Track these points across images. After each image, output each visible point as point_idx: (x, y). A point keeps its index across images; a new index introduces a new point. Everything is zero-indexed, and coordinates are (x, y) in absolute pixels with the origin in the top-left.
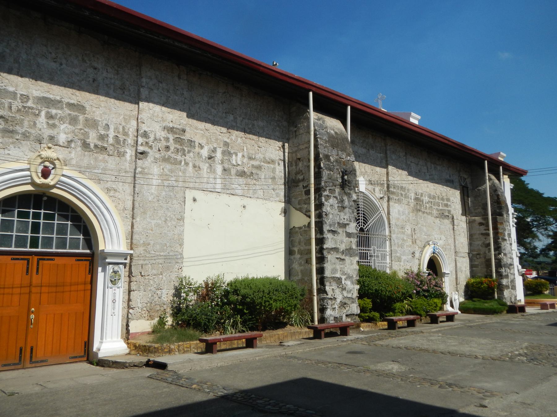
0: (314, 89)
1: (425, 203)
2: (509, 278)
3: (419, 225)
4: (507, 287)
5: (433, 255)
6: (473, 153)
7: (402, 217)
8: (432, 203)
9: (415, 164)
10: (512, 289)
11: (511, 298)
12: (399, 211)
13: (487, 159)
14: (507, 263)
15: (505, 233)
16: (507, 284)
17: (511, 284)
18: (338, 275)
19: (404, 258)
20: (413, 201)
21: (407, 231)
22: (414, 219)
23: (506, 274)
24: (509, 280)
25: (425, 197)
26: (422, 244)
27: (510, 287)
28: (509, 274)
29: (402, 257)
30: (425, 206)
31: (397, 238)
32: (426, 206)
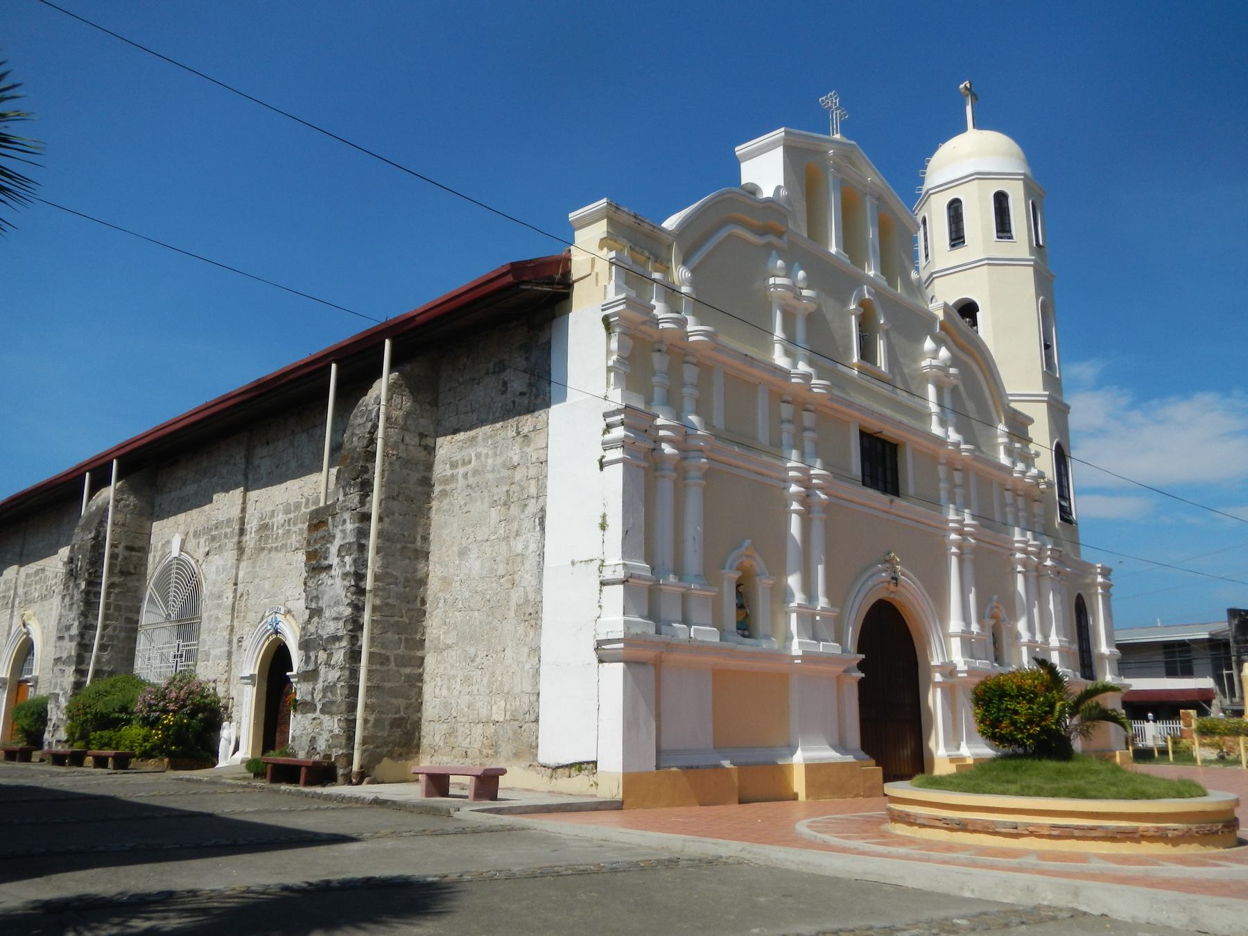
0: (86, 468)
1: (278, 528)
2: (321, 679)
3: (257, 581)
4: (308, 707)
5: (274, 636)
6: (291, 377)
7: (222, 576)
8: (292, 523)
9: (270, 456)
10: (322, 712)
11: (313, 740)
12: (217, 568)
13: (331, 359)
14: (321, 637)
15: (328, 548)
16: (309, 698)
17: (324, 697)
18: (57, 691)
19: (213, 653)
20: (253, 535)
21: (225, 600)
22: (249, 572)
23: (311, 667)
24: (320, 686)
25: (278, 516)
26: (257, 619)
27: (319, 706)
28: (322, 669)
29: (211, 651)
30: (275, 536)
31: (210, 617)
32: (278, 534)
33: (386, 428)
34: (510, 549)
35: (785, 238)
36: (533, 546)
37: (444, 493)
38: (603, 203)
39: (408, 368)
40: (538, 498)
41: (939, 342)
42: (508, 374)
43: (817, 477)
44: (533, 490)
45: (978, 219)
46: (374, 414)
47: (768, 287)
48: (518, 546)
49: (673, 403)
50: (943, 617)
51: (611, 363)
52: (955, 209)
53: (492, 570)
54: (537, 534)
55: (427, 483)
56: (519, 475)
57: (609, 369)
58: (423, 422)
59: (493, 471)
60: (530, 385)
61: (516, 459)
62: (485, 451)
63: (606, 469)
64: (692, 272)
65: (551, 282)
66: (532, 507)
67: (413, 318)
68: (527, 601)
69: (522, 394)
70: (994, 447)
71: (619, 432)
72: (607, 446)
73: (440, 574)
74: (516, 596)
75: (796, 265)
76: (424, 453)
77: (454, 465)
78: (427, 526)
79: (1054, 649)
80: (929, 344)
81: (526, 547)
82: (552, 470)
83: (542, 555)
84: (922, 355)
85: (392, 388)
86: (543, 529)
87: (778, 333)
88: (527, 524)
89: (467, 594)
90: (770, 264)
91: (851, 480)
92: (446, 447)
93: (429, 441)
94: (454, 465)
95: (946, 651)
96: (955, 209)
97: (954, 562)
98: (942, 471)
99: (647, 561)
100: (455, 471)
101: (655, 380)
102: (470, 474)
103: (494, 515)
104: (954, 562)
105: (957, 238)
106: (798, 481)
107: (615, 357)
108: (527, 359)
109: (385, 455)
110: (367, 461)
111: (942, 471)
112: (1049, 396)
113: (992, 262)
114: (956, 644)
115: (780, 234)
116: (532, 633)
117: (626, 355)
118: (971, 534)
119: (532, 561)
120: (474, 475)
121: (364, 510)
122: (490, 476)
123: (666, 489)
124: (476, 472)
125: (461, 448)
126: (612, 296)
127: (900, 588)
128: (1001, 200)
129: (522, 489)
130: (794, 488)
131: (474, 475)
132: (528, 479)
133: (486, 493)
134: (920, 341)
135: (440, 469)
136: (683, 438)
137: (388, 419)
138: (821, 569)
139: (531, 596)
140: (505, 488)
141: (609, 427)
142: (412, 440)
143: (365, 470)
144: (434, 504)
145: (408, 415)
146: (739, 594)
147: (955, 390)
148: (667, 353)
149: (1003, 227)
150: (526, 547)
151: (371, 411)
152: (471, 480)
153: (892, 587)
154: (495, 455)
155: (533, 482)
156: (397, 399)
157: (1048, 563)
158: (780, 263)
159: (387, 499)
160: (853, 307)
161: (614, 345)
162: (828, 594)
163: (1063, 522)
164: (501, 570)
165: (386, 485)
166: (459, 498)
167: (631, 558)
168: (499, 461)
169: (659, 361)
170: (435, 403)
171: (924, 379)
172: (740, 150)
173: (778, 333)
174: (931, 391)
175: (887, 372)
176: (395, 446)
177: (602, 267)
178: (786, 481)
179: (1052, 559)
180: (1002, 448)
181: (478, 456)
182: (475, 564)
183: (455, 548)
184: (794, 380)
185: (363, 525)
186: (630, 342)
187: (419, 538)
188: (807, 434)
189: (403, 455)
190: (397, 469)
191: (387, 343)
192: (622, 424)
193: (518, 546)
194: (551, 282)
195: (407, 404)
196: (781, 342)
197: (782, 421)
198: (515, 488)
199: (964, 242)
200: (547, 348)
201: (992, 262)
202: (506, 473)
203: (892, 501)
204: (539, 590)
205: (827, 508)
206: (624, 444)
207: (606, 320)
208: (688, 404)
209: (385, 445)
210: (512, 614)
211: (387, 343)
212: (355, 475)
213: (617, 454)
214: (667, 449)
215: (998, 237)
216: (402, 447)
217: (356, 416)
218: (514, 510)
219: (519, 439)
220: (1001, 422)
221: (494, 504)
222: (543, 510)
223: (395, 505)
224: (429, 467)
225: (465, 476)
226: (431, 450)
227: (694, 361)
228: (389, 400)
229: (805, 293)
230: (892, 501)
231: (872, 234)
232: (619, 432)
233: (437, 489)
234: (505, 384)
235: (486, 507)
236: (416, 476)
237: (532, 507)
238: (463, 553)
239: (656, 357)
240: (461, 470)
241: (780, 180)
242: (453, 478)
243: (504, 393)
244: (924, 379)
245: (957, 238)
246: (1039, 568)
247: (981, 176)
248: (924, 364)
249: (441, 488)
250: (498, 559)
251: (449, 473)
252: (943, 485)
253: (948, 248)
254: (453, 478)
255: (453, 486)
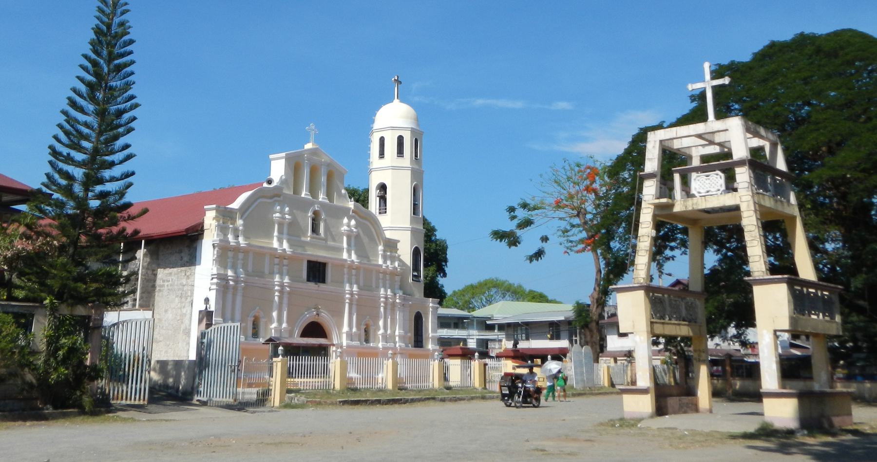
33: (142, 269)
34: (181, 311)
35: (282, 197)
36: (189, 312)
37: (160, 290)
38: (214, 206)
39: (149, 248)
40: (191, 296)
41: (350, 219)
42: (183, 254)
43: (286, 283)
44: (189, 294)
45: (391, 147)
46: (138, 264)
47: (273, 217)
48: (184, 311)
49: (234, 268)
50: (340, 326)
51: (214, 258)
52: (382, 140)
53: (175, 318)
54: (190, 308)
55: (154, 286)
56: (185, 288)
57: (214, 260)
58: (154, 266)
59: (177, 286)
60: (190, 260)
61: (184, 283)
62: (174, 278)
63: (211, 291)
64: (244, 220)
65: (197, 231)
66: (189, 299)
67: (152, 236)
68: (186, 328)
69: (187, 262)
70: (377, 255)
71: (215, 281)
72: (212, 284)
73: (158, 317)
74: (183, 327)
75: (286, 205)
76: (153, 276)
77: (164, 281)
78: (154, 301)
79: (397, 336)
80: (345, 220)
81: (187, 312)
82: (196, 289)
83: (191, 314)
84: (342, 225)
85: (145, 255)
86: (192, 306)
87: (276, 233)
88: (187, 305)
89: (167, 325)
90: (275, 208)
91: (303, 282)
92: (162, 273)
93: (155, 272)
94: (164, 281)
95: (341, 338)
96: (382, 140)
97: (347, 306)
98: (346, 270)
99: (222, 318)
100: (164, 283)
101: (229, 260)
102: (169, 285)
103: (177, 300)
104: (347, 306)
105: (382, 154)
106: (278, 285)
107: (215, 256)
108: (189, 251)
109: (142, 278)
110: (135, 281)
111: (346, 270)
112: (412, 228)
113: (394, 168)
114: (344, 336)
115: (278, 196)
116: (187, 338)
117: (219, 255)
118: (356, 294)
119: (188, 316)
120: (170, 286)
121: (135, 297)
122: (176, 287)
123: (230, 296)
124: (171, 285)
125: (166, 276)
126: (215, 238)
127: (320, 317)
128: (400, 140)
129: (186, 293)
130: (277, 288)
131: (170, 286)
132: (188, 290)
133: (174, 293)
134: (342, 218)
135: (159, 282)
136: (236, 280)
137: (143, 266)
138: (285, 313)
139: (187, 327)
140: (181, 292)
141: (212, 279)
142: (150, 272)
143: (135, 284)
144: (156, 294)
145: (149, 264)
146: (254, 324)
147: (358, 236)
148: (233, 251)
149: (400, 152)
150: (187, 312)
151: (137, 264)
152: (170, 287)
153: (317, 317)
154: (178, 280)
155: (190, 292)
156: (145, 259)
157: (398, 301)
158: (278, 208)
159: (142, 293)
160: (309, 215)
161: (215, 252)
162: (288, 322)
163: (413, 282)
164: (178, 318)
165: (142, 288)
166: (165, 293)
167: (217, 318)
168: (179, 282)
169: (230, 254)
170: (158, 259)
171: (342, 234)
172: (271, 156)
173: (276, 233)
174: (345, 238)
175: (324, 236)
176: (144, 275)
177: (213, 227)
178: (274, 285)
179: (399, 299)
180: (380, 256)
181: (172, 279)
182: (170, 315)
183: (164, 309)
184: (279, 251)
185: (135, 303)
186: (221, 251)
187: (151, 305)
188: (285, 267)
189: (147, 278)
190: (145, 281)
191: (143, 241)
192: (216, 278)
193: (184, 311)
194: (197, 231)
195: (148, 260)
196: (277, 236)
197: (275, 265)
198: (184, 292)
199: (384, 157)
200: (196, 249)
201: (394, 168)
202: (181, 287)
203: (319, 286)
204: (190, 325)
205: (289, 293)
206: (217, 284)
207: (213, 244)
208: (239, 266)
209: (142, 275)
210: (181, 332)
211: (143, 241)
212: (132, 286)
213: (214, 287)
214: (231, 283)
215: (398, 157)
216: (147, 275)
217: (131, 265)
218: (183, 299)
219: (186, 277)
220: (381, 245)
221: (177, 296)
222: (192, 301)
223: (144, 295)
224: (155, 281)
225: (168, 286)
226: (155, 275)
227: (242, 251)
228: (143, 260)
229: (287, 216)
230: (319, 286)
231: (323, 179)
232: (215, 281)
233: (158, 288)
234: (182, 257)
235: (174, 297)
236: (151, 284)
237: (189, 299)
238: (166, 311)
239: (229, 253)
240: (166, 284)
241: (283, 173)
242: (163, 286)
243: (181, 260)
244: (342, 234)
245: (382, 154)
246: (394, 304)
247: (393, 128)
248: (342, 229)
249: (159, 288)
250: (178, 314)
251: (162, 283)
252: (346, 277)
253: (378, 158)
254: (163, 286)
255: (163, 288)
